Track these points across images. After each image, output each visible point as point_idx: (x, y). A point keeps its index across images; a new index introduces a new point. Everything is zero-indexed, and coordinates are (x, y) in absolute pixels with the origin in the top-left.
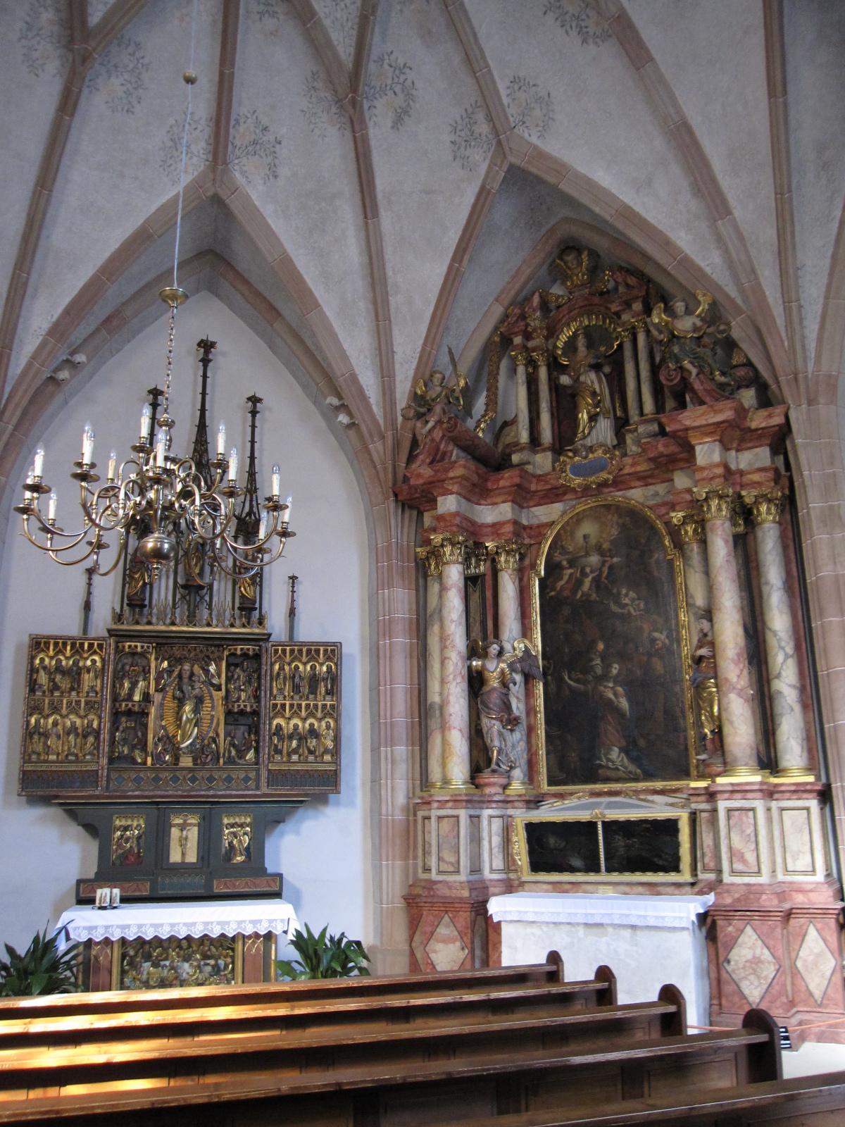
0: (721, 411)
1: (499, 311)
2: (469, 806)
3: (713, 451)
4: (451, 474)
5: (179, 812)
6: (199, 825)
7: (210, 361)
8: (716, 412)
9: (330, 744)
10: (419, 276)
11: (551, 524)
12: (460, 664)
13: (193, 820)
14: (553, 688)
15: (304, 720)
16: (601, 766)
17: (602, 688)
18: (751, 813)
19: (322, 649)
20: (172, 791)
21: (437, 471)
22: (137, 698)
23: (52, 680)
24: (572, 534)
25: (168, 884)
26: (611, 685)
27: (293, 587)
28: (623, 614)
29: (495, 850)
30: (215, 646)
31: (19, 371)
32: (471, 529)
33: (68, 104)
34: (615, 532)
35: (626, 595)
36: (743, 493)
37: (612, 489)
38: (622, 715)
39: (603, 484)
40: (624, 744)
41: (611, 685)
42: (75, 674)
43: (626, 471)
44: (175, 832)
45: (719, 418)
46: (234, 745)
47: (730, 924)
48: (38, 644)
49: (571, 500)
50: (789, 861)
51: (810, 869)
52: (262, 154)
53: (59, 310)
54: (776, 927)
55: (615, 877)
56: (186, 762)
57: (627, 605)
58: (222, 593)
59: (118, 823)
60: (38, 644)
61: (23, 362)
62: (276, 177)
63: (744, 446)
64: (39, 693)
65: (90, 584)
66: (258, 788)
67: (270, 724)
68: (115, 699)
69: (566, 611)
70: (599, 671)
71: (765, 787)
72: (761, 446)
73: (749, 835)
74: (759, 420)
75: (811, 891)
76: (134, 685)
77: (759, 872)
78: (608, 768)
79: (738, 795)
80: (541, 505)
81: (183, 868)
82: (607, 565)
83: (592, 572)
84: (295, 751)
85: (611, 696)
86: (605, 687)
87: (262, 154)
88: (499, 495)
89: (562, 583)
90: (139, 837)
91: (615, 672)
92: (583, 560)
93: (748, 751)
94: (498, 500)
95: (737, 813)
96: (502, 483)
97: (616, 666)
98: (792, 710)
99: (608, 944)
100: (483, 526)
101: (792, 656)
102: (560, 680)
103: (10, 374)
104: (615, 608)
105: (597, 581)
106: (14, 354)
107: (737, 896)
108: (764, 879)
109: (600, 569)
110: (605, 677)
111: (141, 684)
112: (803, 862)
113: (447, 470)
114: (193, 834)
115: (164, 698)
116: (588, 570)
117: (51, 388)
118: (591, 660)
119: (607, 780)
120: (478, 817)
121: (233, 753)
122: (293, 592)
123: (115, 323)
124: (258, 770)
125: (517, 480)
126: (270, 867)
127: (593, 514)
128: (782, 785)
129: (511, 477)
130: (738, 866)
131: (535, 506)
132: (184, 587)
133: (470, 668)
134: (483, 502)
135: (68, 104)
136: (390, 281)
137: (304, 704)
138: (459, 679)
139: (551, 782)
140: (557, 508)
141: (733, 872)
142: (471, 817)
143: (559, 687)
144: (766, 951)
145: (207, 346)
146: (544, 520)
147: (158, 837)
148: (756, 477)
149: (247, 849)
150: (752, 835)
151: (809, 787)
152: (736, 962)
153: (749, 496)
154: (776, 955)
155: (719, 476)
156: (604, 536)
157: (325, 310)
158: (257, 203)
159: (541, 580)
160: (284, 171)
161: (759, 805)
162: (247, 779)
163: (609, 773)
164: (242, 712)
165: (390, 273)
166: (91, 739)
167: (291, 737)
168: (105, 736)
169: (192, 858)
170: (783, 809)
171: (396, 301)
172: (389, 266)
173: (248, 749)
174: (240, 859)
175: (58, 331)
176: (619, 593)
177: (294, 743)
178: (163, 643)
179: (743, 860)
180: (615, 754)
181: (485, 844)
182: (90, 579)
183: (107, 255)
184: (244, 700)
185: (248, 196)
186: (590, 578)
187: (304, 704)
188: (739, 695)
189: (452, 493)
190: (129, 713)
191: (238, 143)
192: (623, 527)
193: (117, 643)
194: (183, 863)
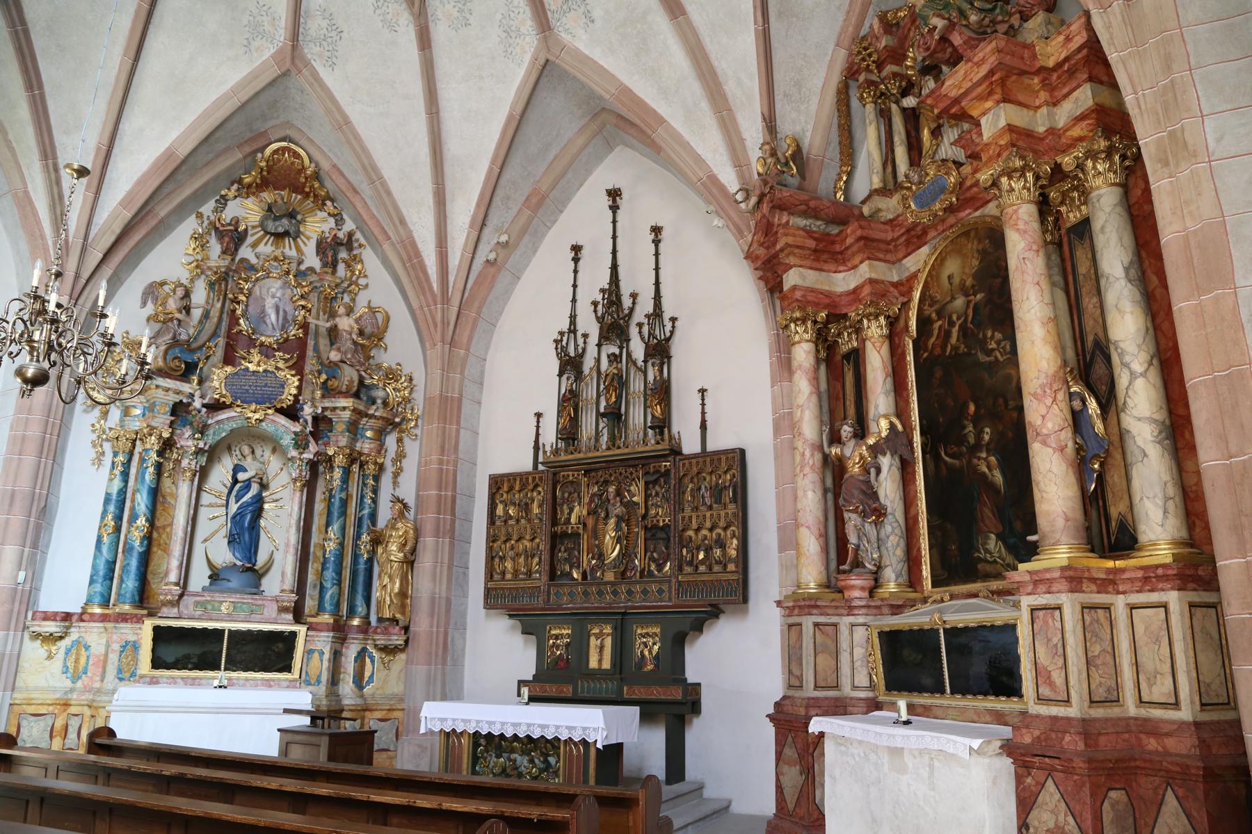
0: (983, 60)
1: (843, 53)
2: (815, 611)
3: (998, 116)
4: (778, 247)
5: (596, 622)
6: (612, 634)
7: (618, 208)
8: (978, 65)
9: (733, 553)
10: (737, 56)
11: (914, 276)
12: (808, 453)
13: (608, 630)
14: (931, 466)
15: (711, 530)
16: (980, 560)
17: (975, 461)
18: (1057, 612)
19: (723, 458)
20: (594, 603)
21: (767, 248)
22: (573, 520)
23: (506, 512)
24: (938, 277)
25: (584, 687)
26: (984, 455)
27: (703, 399)
28: (990, 363)
29: (857, 664)
30: (633, 466)
31: (457, 263)
32: (827, 301)
33: (425, 41)
34: (976, 263)
35: (992, 337)
36: (1059, 160)
37: (967, 211)
38: (999, 491)
39: (950, 209)
40: (1001, 529)
41: (984, 455)
42: (526, 507)
43: (968, 183)
44: (593, 642)
45: (984, 70)
46: (654, 560)
47: (1029, 774)
48: (496, 483)
49: (934, 238)
50: (1144, 686)
51: (1172, 700)
52: (575, 7)
53: (474, 204)
54: (1083, 785)
55: (959, 702)
56: (610, 576)
57: (993, 350)
58: (637, 416)
59: (553, 632)
60: (497, 483)
61: (458, 255)
62: (593, 21)
63: (1059, 94)
64: (498, 523)
65: (538, 427)
66: (670, 600)
67: (681, 537)
68: (554, 522)
69: (938, 373)
70: (972, 440)
71: (1068, 573)
72: (1078, 86)
73: (1056, 646)
74: (1053, 52)
75: (1168, 735)
76: (571, 510)
77: (1067, 702)
78: (988, 562)
79: (1042, 588)
80: (909, 254)
81: (599, 674)
82: (972, 306)
83: (958, 319)
84: (702, 562)
85: (986, 470)
86: (979, 458)
87: (575, 7)
88: (853, 255)
89: (932, 340)
90: (568, 645)
91: (987, 437)
92: (950, 307)
93: (1060, 522)
94: (857, 260)
95: (1041, 613)
96: (849, 241)
97: (987, 430)
98: (1145, 455)
99: (909, 785)
100: (841, 295)
101: (1144, 375)
102: (937, 458)
104: (983, 358)
105: (963, 329)
107: (1037, 733)
108: (1073, 712)
109: (966, 314)
110: (977, 447)
111: (577, 509)
112: (1160, 690)
113: (774, 244)
114: (608, 642)
115: (597, 521)
116: (954, 318)
117: (492, 270)
118: (964, 427)
119: (987, 577)
120: (835, 625)
121: (653, 567)
122: (703, 405)
123: (534, 200)
124: (670, 581)
125: (859, 233)
126: (691, 676)
127: (954, 247)
128: (1123, 570)
129: (854, 232)
130: (1045, 691)
131: (905, 257)
132: (603, 415)
133: (826, 458)
134: (841, 268)
135: (425, 41)
136: (719, 71)
137: (708, 515)
138: (807, 470)
139: (935, 584)
140: (925, 250)
141: (1040, 699)
142: (816, 625)
143: (937, 467)
144: (1070, 819)
145: (614, 194)
146: (913, 269)
147: (579, 645)
148: (1076, 132)
149: (657, 657)
150: (1060, 645)
151: (1160, 571)
152: (1036, 829)
153: (1067, 161)
154: (1082, 826)
155: (1006, 147)
156: (967, 270)
157: (672, 123)
158: (587, 52)
159: (914, 342)
160: (597, 13)
161: (1069, 602)
162: (660, 591)
163: (988, 568)
164: (655, 527)
165: (715, 64)
166: (536, 560)
167: (698, 549)
168: (546, 557)
169: (606, 665)
170: (1133, 607)
171: (730, 88)
172: (712, 57)
173: (665, 563)
174: (650, 667)
175: (481, 224)
176: (985, 336)
177: (701, 556)
178: (590, 469)
179: (1051, 684)
180: (992, 543)
181: (845, 658)
182: (538, 422)
183: (493, 146)
184: (661, 515)
185: (577, 50)
186: (957, 327)
187: (708, 515)
188: (1044, 443)
189: (791, 267)
190: (565, 535)
191: (553, 8)
192: (983, 254)
193: (555, 474)
194: (600, 669)
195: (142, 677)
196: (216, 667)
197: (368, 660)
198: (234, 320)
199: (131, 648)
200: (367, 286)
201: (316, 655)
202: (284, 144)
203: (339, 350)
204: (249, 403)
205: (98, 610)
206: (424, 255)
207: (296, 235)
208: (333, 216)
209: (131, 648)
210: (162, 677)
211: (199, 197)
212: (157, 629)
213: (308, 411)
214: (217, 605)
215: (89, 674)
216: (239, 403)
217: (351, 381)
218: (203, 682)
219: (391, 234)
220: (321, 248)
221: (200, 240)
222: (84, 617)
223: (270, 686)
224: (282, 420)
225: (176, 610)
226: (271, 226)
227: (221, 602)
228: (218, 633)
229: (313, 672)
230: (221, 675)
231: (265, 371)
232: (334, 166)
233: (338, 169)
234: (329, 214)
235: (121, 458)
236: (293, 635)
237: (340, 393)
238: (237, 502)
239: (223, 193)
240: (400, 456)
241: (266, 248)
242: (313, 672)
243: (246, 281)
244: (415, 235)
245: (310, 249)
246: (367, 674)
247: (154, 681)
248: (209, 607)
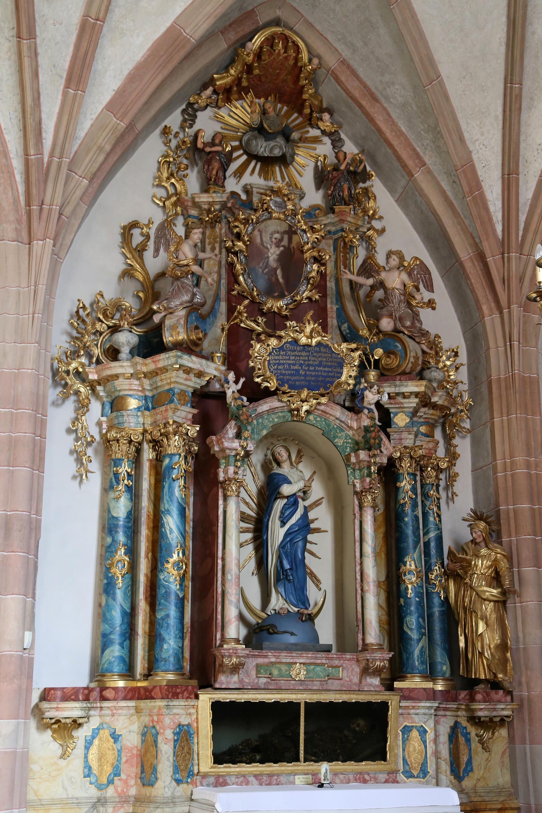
103: (521, 201)
106: (521, 177)
195: (205, 776)
196: (297, 760)
197: (462, 740)
198: (233, 278)
199: (184, 736)
200: (383, 230)
201: (415, 734)
202: (278, 29)
203: (390, 316)
204: (299, 388)
205: (121, 684)
206: (485, 186)
207: (284, 161)
208: (330, 135)
209: (184, 736)
210: (229, 774)
211: (167, 109)
212: (217, 708)
213: (371, 397)
214: (284, 668)
215: (123, 776)
216: (285, 388)
217: (416, 358)
218: (282, 779)
219: (427, 159)
220: (321, 178)
221: (170, 167)
222: (107, 693)
223: (365, 781)
224: (338, 412)
225: (235, 678)
226: (262, 147)
227: (291, 664)
228: (293, 706)
229: (415, 759)
230: (300, 770)
231: (319, 344)
232: (344, 62)
233: (349, 67)
234: (324, 132)
235: (125, 468)
236: (384, 706)
237: (404, 373)
238: (283, 523)
239: (192, 100)
240: (452, 456)
241: (253, 178)
242: (415, 759)
243: (246, 222)
244: (475, 157)
245: (306, 180)
246: (464, 759)
247: (220, 782)
248: (275, 672)
